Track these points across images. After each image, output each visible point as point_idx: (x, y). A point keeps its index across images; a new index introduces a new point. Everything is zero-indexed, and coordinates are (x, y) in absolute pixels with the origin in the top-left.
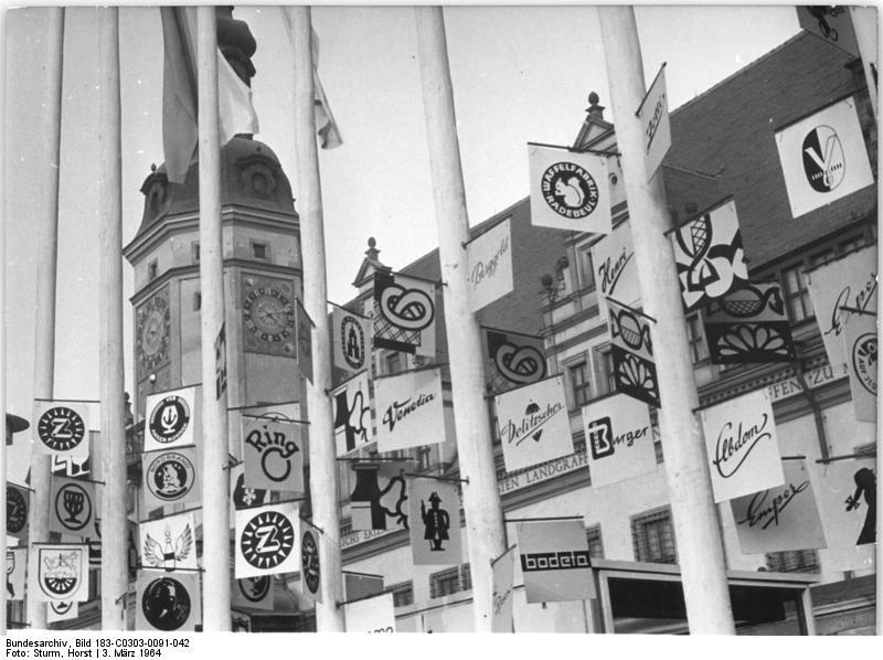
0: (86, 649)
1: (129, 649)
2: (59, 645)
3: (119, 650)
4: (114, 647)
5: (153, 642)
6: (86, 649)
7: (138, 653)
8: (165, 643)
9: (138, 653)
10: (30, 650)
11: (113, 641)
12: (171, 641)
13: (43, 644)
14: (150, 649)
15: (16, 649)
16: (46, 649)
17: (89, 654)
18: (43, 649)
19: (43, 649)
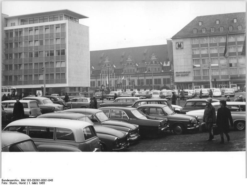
0: (24, 182)
1: (36, 182)
2: (17, 181)
3: (33, 182)
4: (39, 181)
5: (43, 180)
6: (24, 182)
7: (38, 183)
8: (46, 180)
9: (38, 183)
10: (8, 182)
11: (32, 180)
12: (48, 180)
13: (12, 181)
14: (42, 182)
15: (4, 182)
16: (13, 182)
17: (25, 183)
18: (12, 182)
19: (12, 182)
